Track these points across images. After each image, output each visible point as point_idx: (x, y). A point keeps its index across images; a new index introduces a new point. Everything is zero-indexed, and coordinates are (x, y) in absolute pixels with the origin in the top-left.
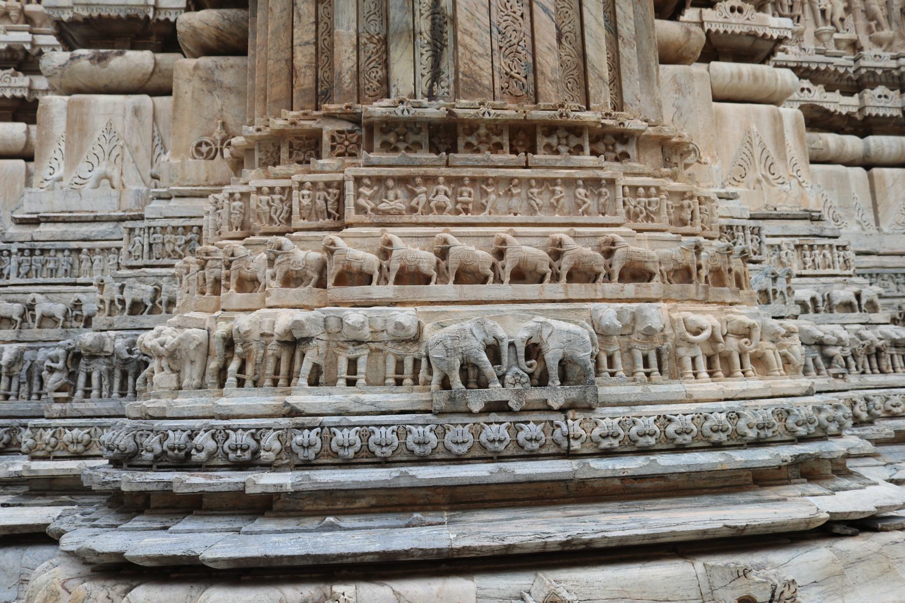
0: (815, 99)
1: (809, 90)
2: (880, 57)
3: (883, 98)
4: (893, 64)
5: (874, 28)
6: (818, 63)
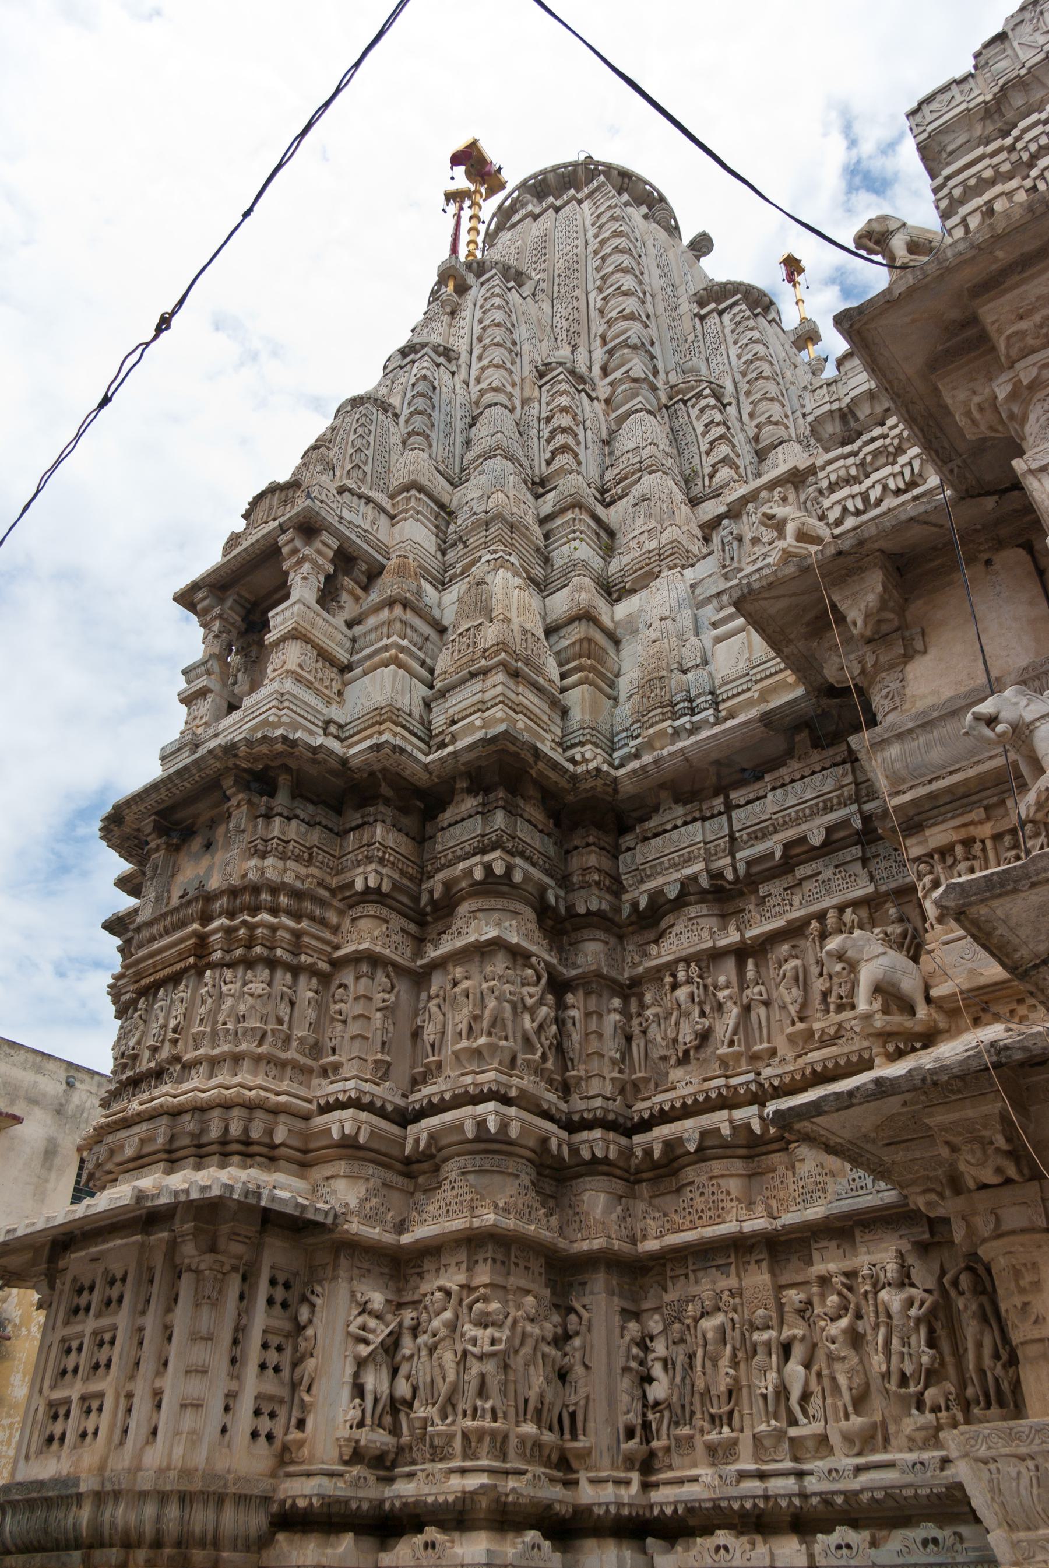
3: (845, 1551)
6: (741, 1498)
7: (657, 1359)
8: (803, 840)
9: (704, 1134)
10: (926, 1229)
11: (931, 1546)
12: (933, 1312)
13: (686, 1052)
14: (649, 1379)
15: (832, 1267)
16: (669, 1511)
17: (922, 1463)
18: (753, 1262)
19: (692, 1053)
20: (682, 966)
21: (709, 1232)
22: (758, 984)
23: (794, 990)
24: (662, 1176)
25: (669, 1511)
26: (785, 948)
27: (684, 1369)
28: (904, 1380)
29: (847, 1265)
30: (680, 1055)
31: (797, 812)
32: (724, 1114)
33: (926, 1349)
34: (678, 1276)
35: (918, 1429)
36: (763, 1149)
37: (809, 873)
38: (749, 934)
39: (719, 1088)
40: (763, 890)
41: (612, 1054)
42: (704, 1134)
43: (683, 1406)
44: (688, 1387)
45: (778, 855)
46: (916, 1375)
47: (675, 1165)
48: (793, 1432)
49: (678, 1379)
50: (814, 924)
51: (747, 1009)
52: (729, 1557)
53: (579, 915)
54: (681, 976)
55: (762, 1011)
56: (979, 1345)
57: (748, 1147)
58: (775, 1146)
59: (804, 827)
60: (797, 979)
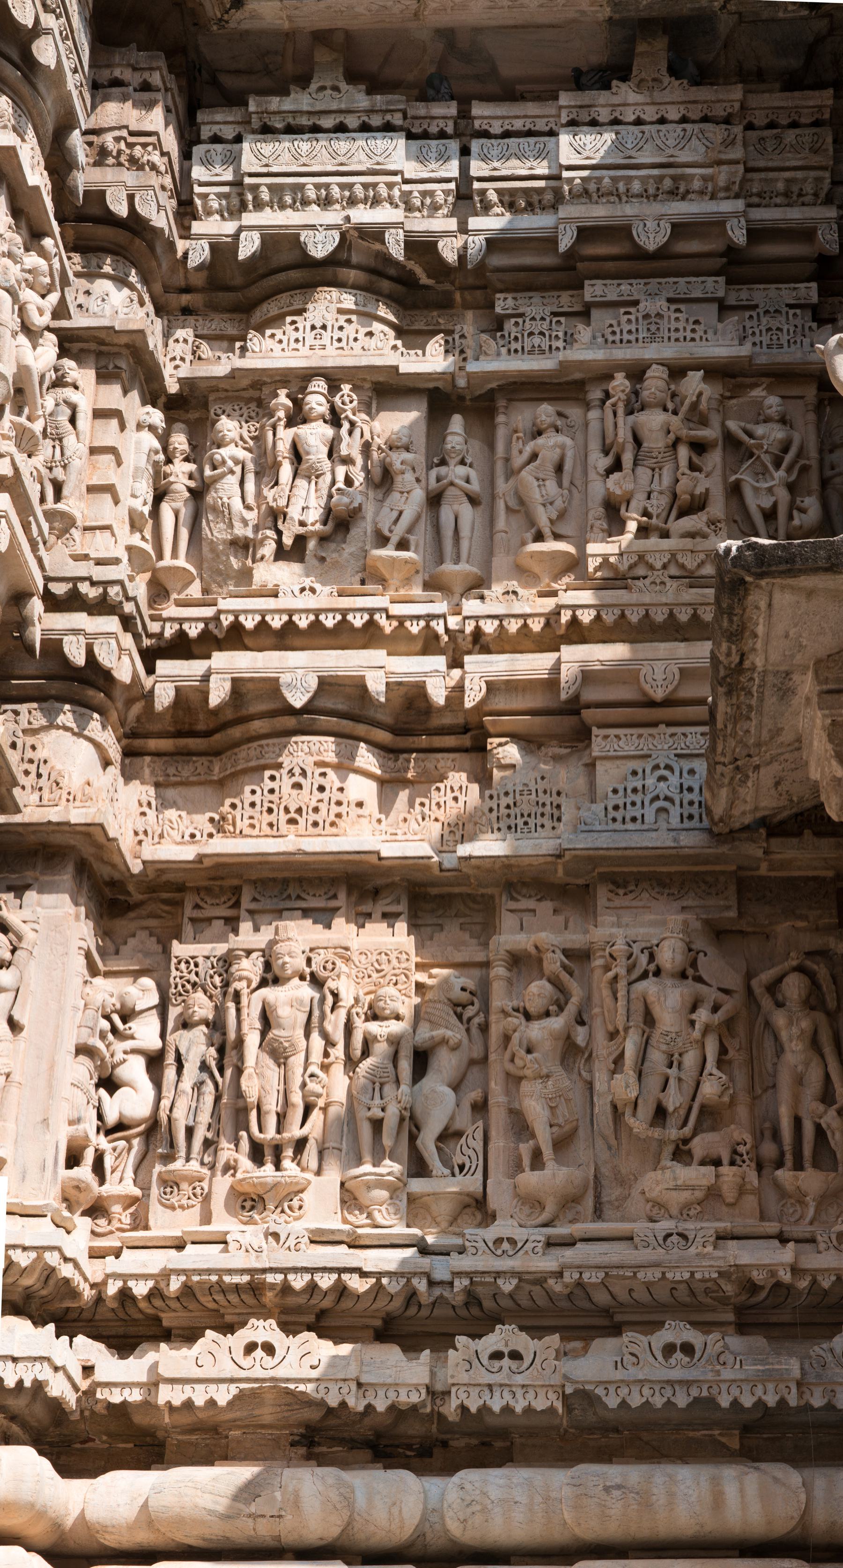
0: (281, 1372)
1: (269, 1349)
2: (512, 1241)
3: (506, 1362)
4: (547, 1263)
5: (526, 1162)
6: (312, 1270)
7: (134, 1051)
8: (620, 232)
9: (326, 684)
10: (733, 902)
11: (678, 1355)
12: (729, 1024)
13: (300, 540)
14: (109, 1083)
15: (546, 937)
16: (140, 1289)
17: (684, 1236)
18: (377, 914)
19: (312, 544)
20: (320, 385)
21: (315, 844)
22: (462, 462)
23: (551, 485)
24: (189, 753)
25: (140, 1289)
26: (545, 412)
27: (204, 1067)
28: (660, 1114)
29: (575, 939)
30: (288, 541)
31: (614, 179)
32: (378, 656)
33: (715, 1071)
34: (209, 920)
35: (676, 1188)
36: (424, 741)
37: (612, 296)
38: (473, 367)
39: (372, 611)
40: (503, 304)
41: (137, 504)
42: (326, 684)
43: (190, 1132)
44: (209, 1099)
45: (565, 243)
46: (683, 1112)
47: (236, 732)
48: (417, 1185)
49: (187, 1084)
50: (620, 383)
51: (434, 500)
52: (269, 1361)
53: (110, 219)
54: (316, 401)
55: (466, 511)
56: (799, 1081)
57: (396, 731)
58: (450, 741)
59: (629, 210)
60: (559, 469)
